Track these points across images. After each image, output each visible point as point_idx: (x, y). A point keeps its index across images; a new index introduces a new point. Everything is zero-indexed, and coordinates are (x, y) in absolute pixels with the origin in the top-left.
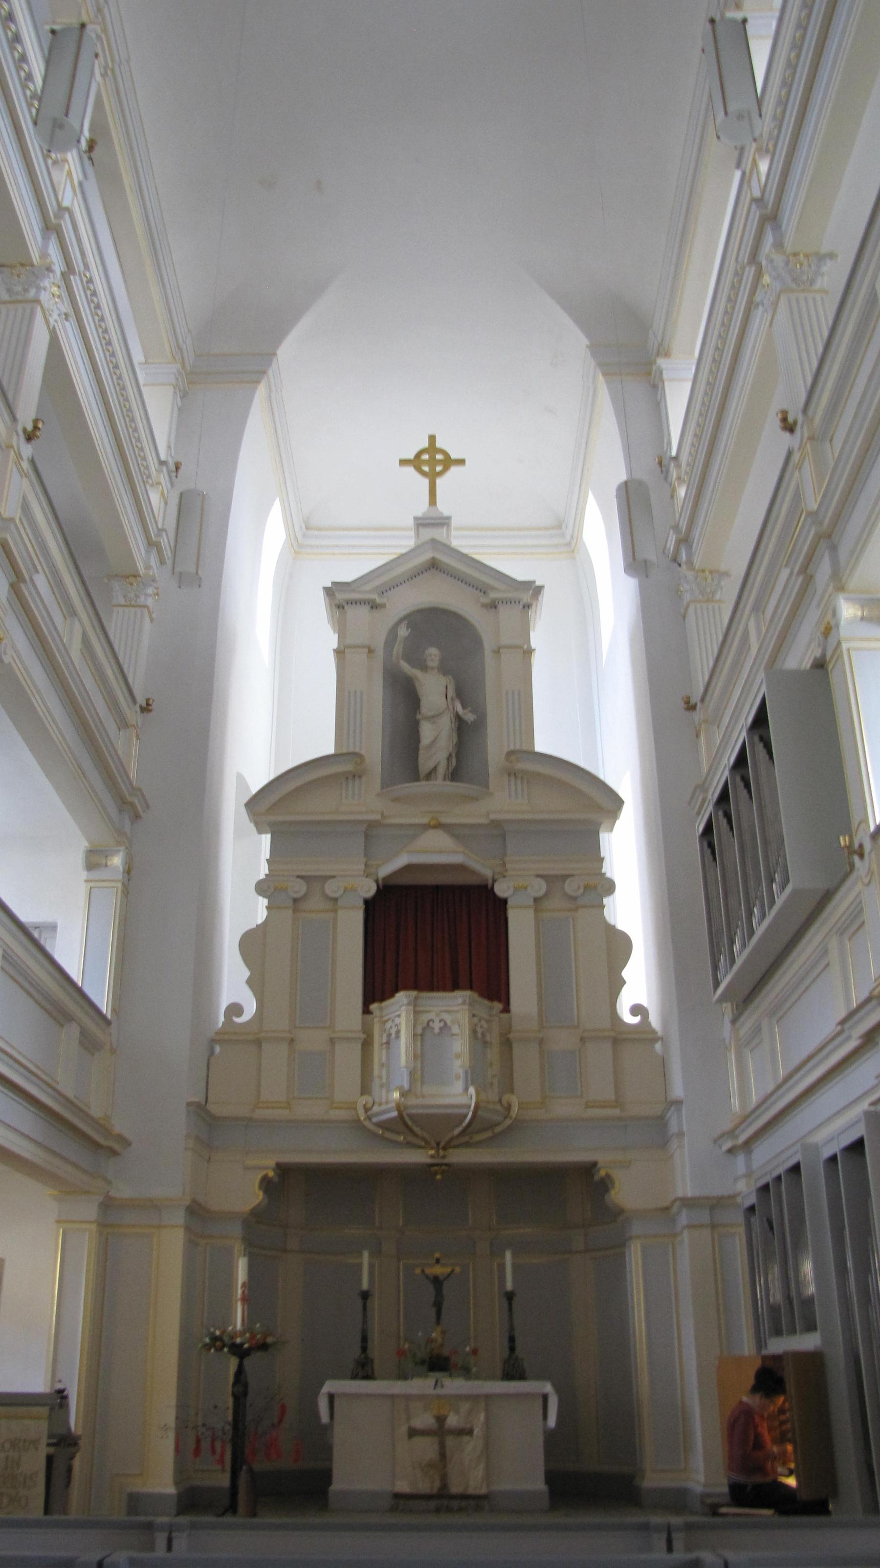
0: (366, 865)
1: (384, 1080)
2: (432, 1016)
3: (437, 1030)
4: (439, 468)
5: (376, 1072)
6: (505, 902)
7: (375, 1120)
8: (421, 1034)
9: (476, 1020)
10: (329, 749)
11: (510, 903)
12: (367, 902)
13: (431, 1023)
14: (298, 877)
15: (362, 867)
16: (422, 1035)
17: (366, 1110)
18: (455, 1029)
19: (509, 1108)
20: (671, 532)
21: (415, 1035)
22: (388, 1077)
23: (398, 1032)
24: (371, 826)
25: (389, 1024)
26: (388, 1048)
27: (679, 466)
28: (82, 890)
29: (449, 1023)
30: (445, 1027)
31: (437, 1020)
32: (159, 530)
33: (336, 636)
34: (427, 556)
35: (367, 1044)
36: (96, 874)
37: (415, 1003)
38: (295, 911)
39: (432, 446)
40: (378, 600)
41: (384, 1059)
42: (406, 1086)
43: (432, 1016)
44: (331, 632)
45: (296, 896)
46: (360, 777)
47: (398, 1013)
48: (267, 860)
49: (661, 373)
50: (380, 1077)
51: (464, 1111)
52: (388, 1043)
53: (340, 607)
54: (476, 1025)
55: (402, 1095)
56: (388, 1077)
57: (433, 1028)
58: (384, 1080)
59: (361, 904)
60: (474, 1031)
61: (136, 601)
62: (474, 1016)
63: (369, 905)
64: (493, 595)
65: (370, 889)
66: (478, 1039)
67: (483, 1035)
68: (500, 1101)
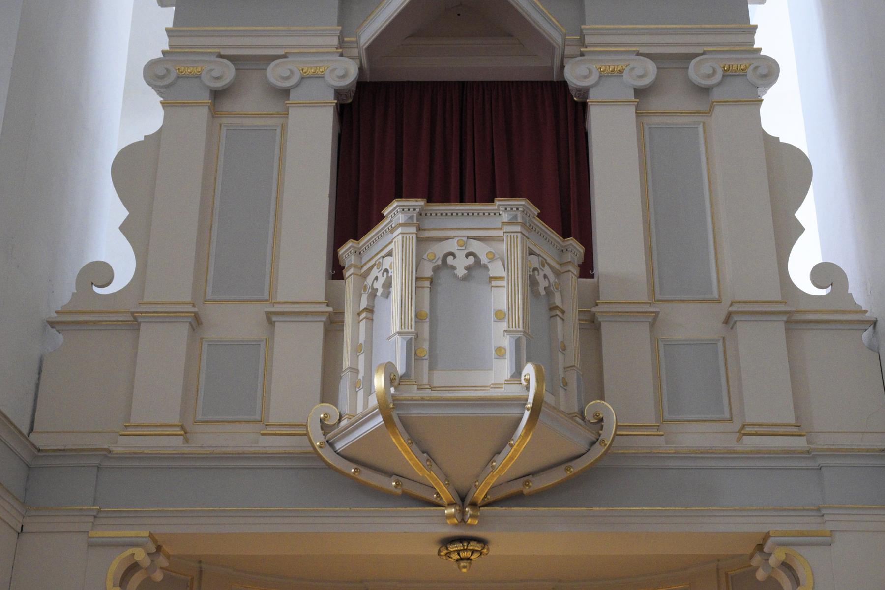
2: (452, 246)
3: (461, 272)
5: (347, 363)
7: (340, 446)
9: (535, 262)
11: (593, 97)
13: (450, 259)
15: (335, 41)
16: (432, 281)
17: (325, 427)
18: (497, 269)
23: (388, 285)
25: (375, 272)
29: (484, 260)
31: (461, 255)
37: (419, 222)
38: (215, 113)
41: (362, 339)
42: (401, 369)
43: (452, 246)
45: (219, 85)
48: (168, 30)
50: (355, 370)
51: (514, 412)
52: (370, 310)
55: (391, 380)
57: (453, 268)
59: (332, 100)
60: (533, 283)
62: (531, 253)
67: (548, 291)
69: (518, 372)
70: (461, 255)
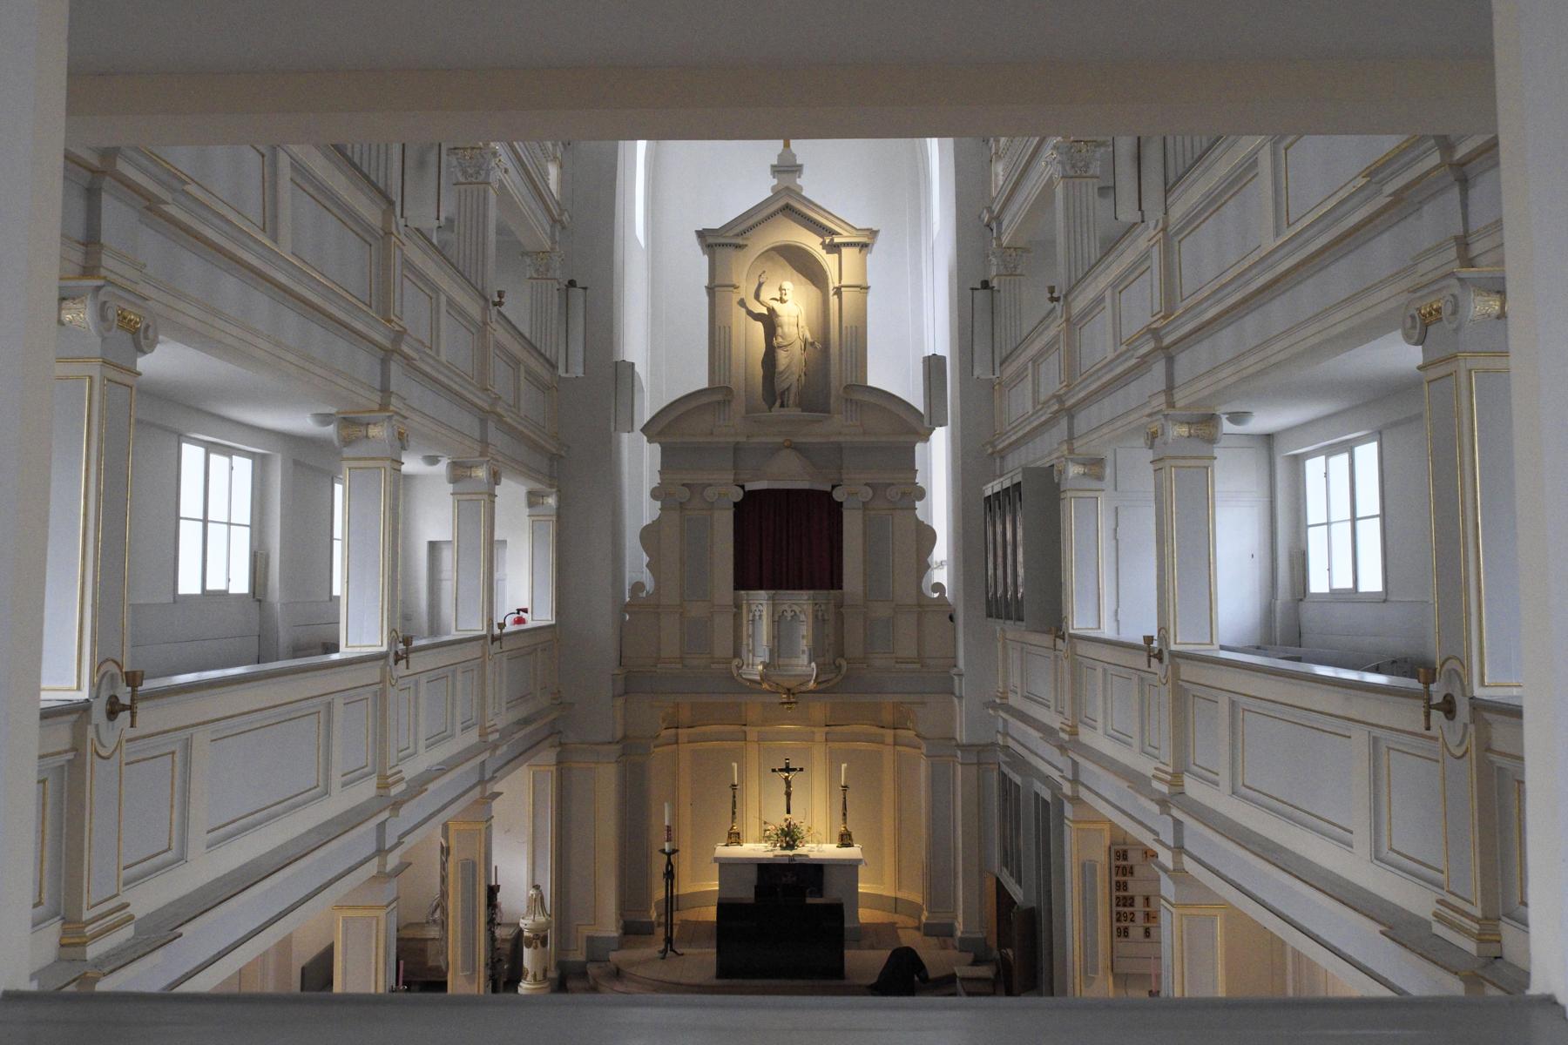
0: (735, 474)
1: (751, 648)
3: (789, 618)
6: (841, 504)
8: (777, 621)
10: (704, 383)
11: (844, 504)
12: (736, 505)
14: (683, 485)
18: (803, 617)
19: (839, 667)
20: (985, 211)
21: (774, 622)
22: (753, 645)
23: (760, 616)
24: (737, 449)
26: (753, 624)
28: (526, 521)
29: (798, 612)
30: (795, 615)
31: (789, 612)
32: (561, 209)
33: (706, 258)
34: (781, 203)
35: (737, 616)
36: (537, 510)
37: (772, 598)
40: (740, 241)
41: (750, 633)
42: (767, 661)
44: (701, 252)
46: (729, 401)
50: (748, 645)
52: (753, 620)
53: (710, 246)
54: (818, 611)
55: (764, 668)
56: (753, 645)
58: (751, 648)
60: (816, 616)
62: (816, 604)
64: (837, 240)
65: (738, 495)
66: (819, 621)
67: (823, 615)
68: (834, 663)
69: (810, 663)
70: (789, 612)
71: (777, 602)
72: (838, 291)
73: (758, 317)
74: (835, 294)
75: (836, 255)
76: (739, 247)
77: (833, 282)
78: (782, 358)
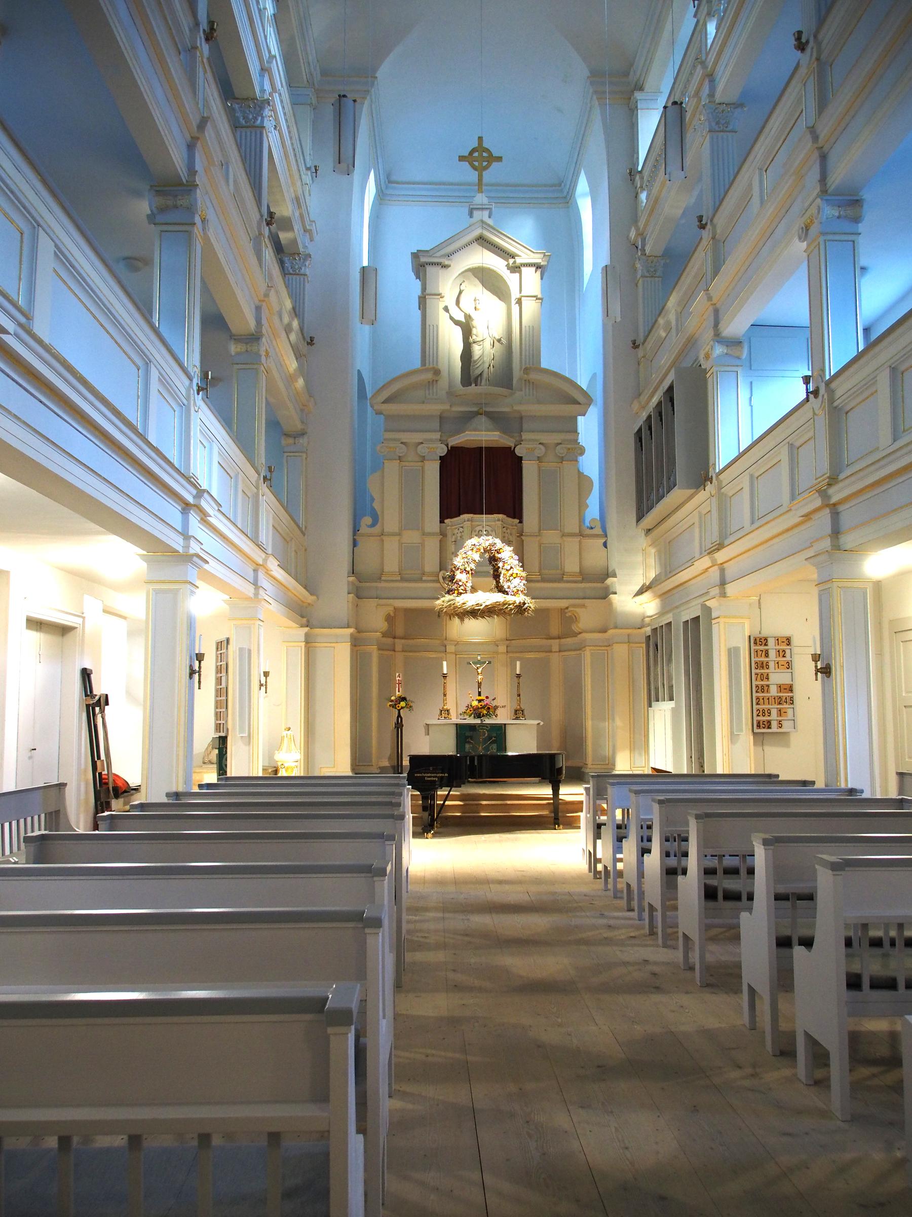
4: (485, 164)
6: (520, 459)
27: (642, 178)
39: (480, 147)
40: (447, 263)
46: (437, 381)
47: (462, 525)
49: (637, 102)
61: (299, 271)
63: (444, 461)
71: (474, 523)
72: (519, 302)
73: (457, 323)
74: (516, 303)
75: (517, 275)
76: (445, 267)
77: (515, 294)
78: (477, 350)
